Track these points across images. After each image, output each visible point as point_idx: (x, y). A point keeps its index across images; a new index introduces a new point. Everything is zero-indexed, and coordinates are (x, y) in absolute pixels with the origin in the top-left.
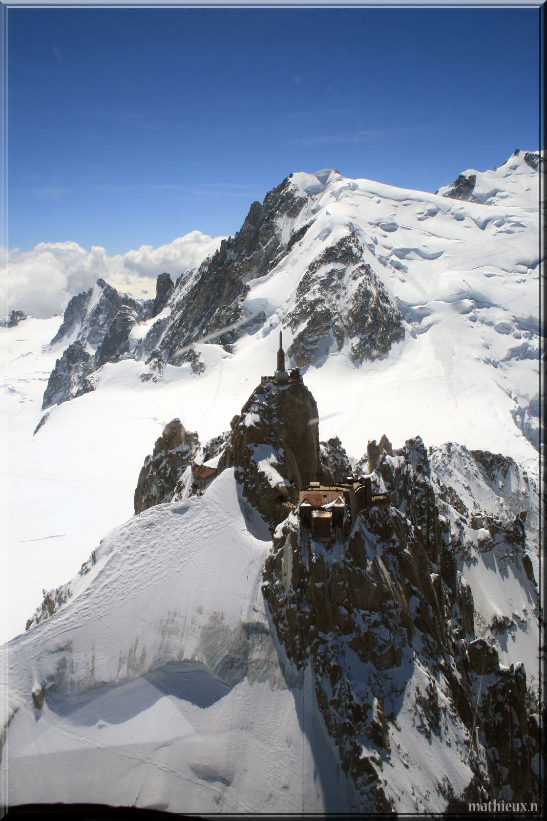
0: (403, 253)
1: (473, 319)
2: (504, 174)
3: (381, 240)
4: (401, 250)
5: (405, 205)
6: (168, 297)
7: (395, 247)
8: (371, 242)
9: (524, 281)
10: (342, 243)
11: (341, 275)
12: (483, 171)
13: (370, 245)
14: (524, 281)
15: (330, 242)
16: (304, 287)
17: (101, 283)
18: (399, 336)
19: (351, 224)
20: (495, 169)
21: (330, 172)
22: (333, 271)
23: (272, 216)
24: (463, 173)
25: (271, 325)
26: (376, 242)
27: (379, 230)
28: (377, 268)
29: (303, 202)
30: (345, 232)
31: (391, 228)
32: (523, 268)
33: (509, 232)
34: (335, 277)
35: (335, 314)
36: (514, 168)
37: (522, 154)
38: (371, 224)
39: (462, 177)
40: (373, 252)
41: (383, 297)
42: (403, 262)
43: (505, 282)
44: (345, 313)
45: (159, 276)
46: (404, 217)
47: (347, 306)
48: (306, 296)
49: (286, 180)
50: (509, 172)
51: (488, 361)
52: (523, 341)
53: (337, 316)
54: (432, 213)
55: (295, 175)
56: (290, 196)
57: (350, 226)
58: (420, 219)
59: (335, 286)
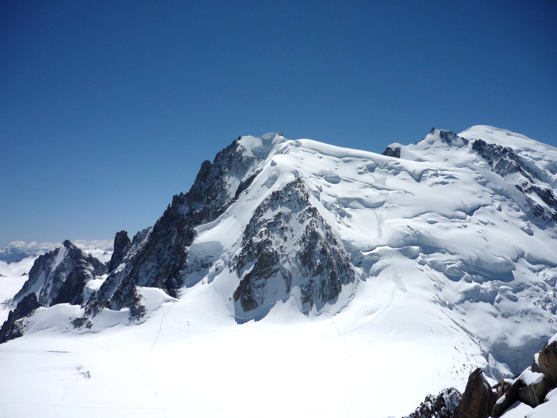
0: (346, 202)
1: (422, 263)
2: (425, 147)
3: (324, 188)
4: (346, 199)
5: (346, 162)
6: (125, 254)
7: (340, 196)
8: (317, 190)
9: (465, 226)
10: (289, 187)
11: (288, 218)
12: (406, 145)
13: (315, 192)
14: (465, 226)
15: (277, 187)
16: (249, 231)
17: (67, 243)
18: (349, 278)
19: (296, 171)
20: (416, 143)
21: (274, 136)
22: (280, 214)
23: (222, 173)
24: (390, 146)
25: (217, 269)
26: (321, 191)
27: (323, 181)
28: (322, 211)
29: (250, 161)
30: (291, 178)
31: (335, 180)
32: (462, 214)
33: (443, 183)
34: (282, 219)
35: (282, 256)
36: (432, 143)
37: (438, 132)
38: (315, 175)
39: (388, 149)
40: (318, 198)
41: (331, 239)
42: (347, 210)
43: (447, 228)
44: (293, 255)
45: (118, 234)
46: (345, 171)
47: (294, 248)
48: (254, 238)
49: (235, 142)
50: (428, 146)
51: (444, 304)
52: (474, 284)
53: (285, 258)
54: (371, 169)
55: (243, 138)
56: (239, 154)
57: (296, 173)
58: (360, 173)
59: (283, 228)
